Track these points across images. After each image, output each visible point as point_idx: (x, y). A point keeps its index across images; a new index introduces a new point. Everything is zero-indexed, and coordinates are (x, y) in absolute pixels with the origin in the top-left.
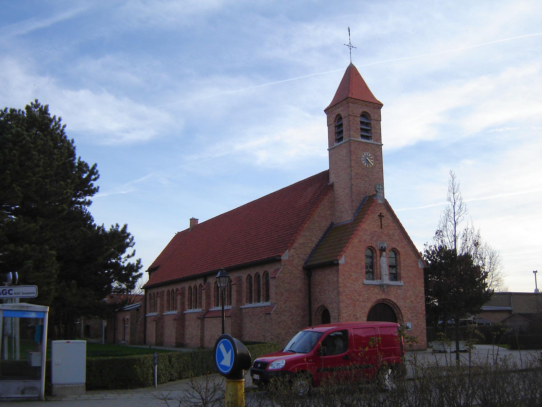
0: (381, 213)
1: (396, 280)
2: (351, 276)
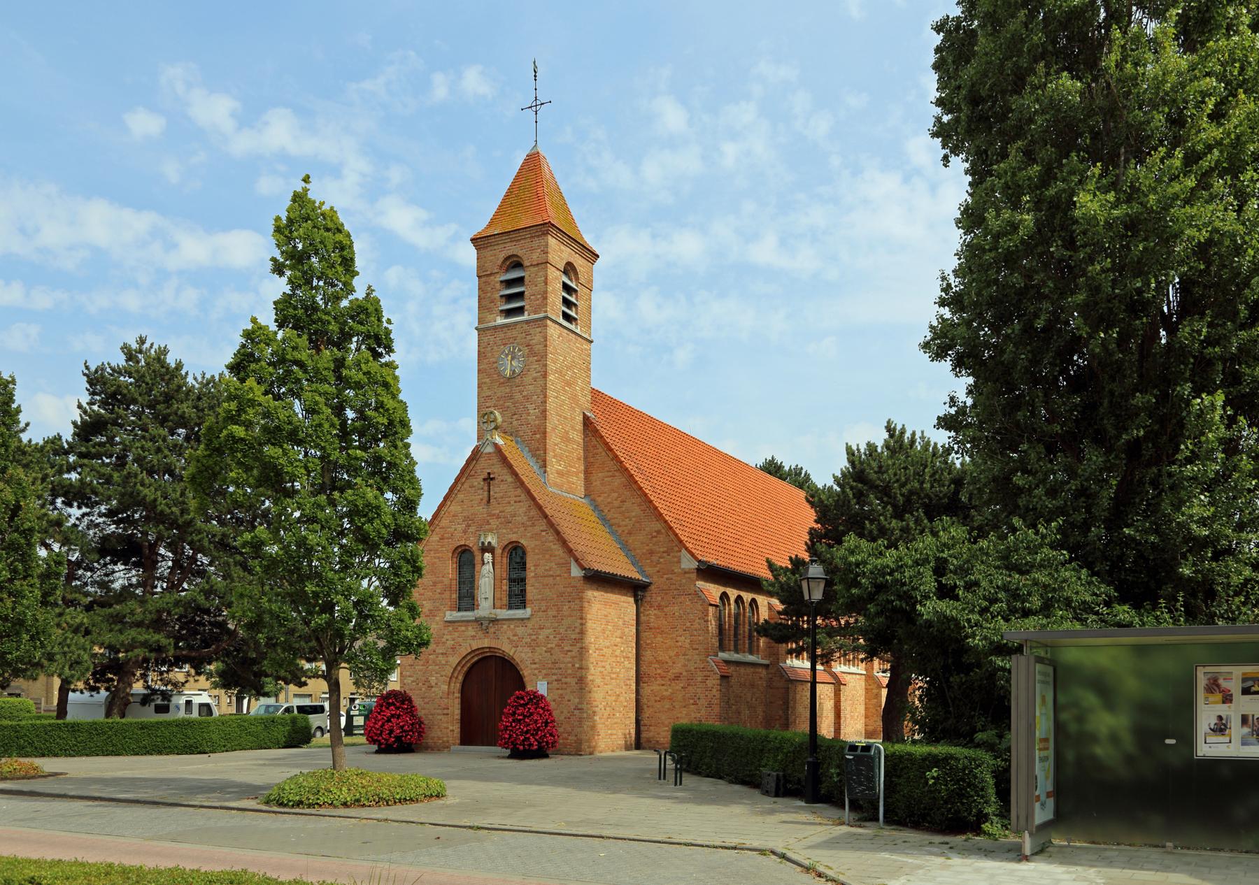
1: (518, 608)
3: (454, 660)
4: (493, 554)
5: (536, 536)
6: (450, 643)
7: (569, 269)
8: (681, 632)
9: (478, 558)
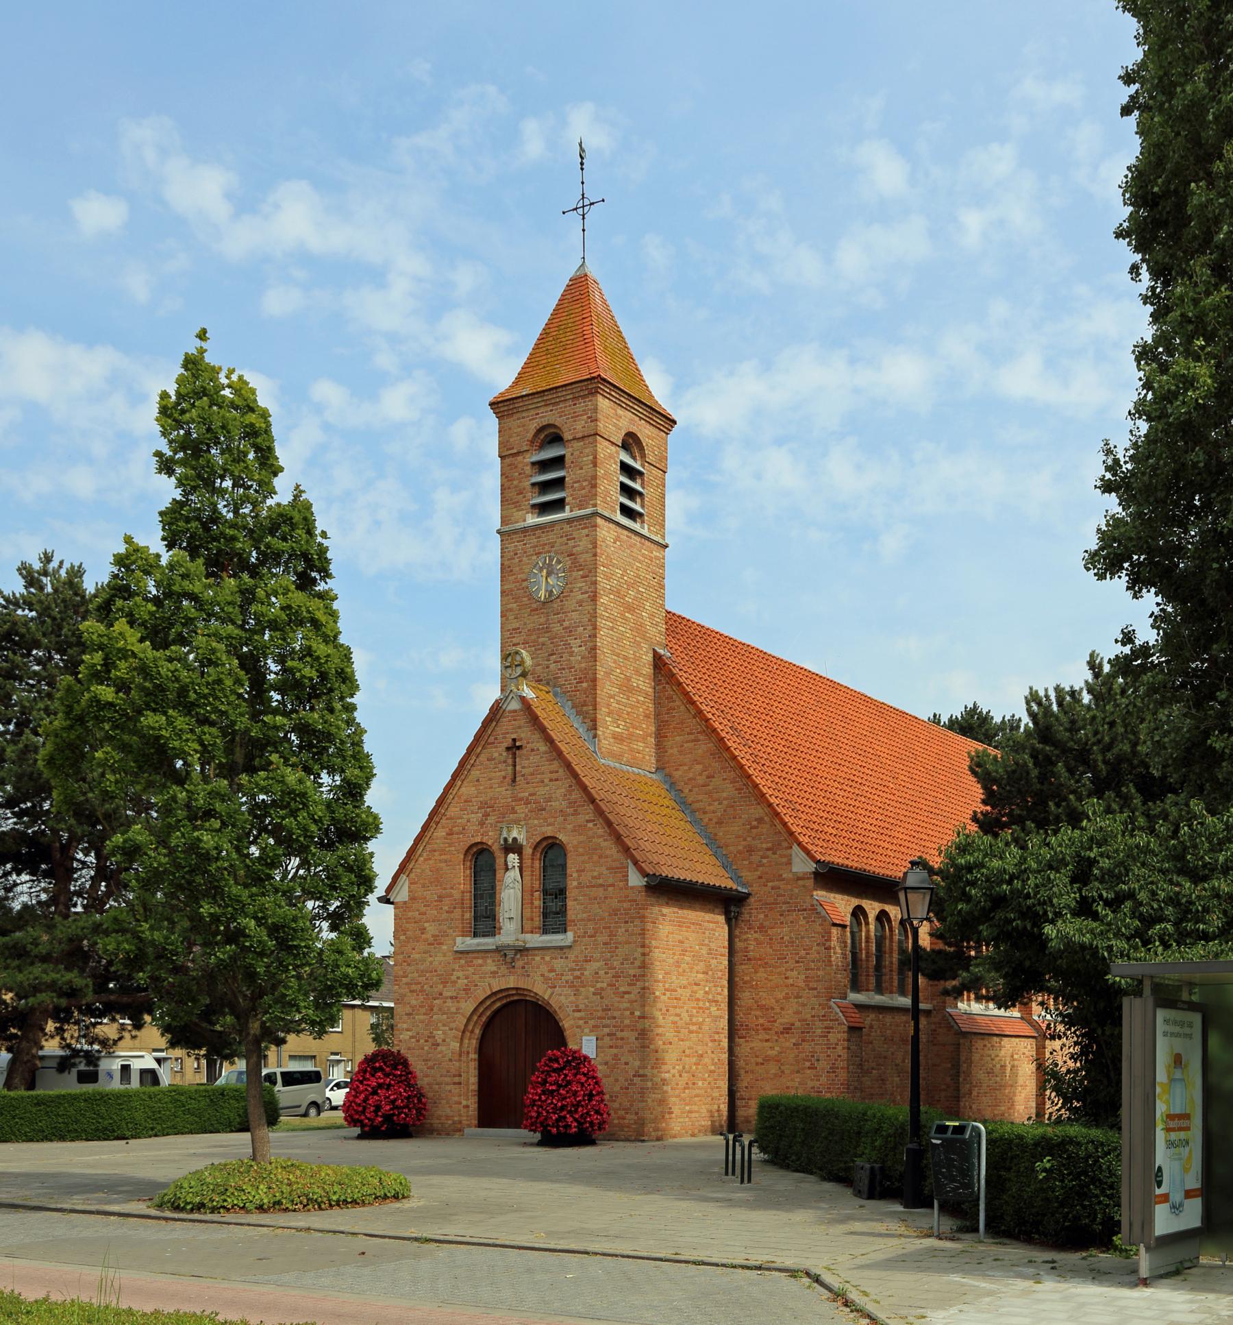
0: (514, 740)
1: (556, 932)
2: (423, 930)
3: (468, 1007)
4: (520, 854)
5: (579, 829)
7: (631, 442)
8: (792, 964)
9: (500, 861)
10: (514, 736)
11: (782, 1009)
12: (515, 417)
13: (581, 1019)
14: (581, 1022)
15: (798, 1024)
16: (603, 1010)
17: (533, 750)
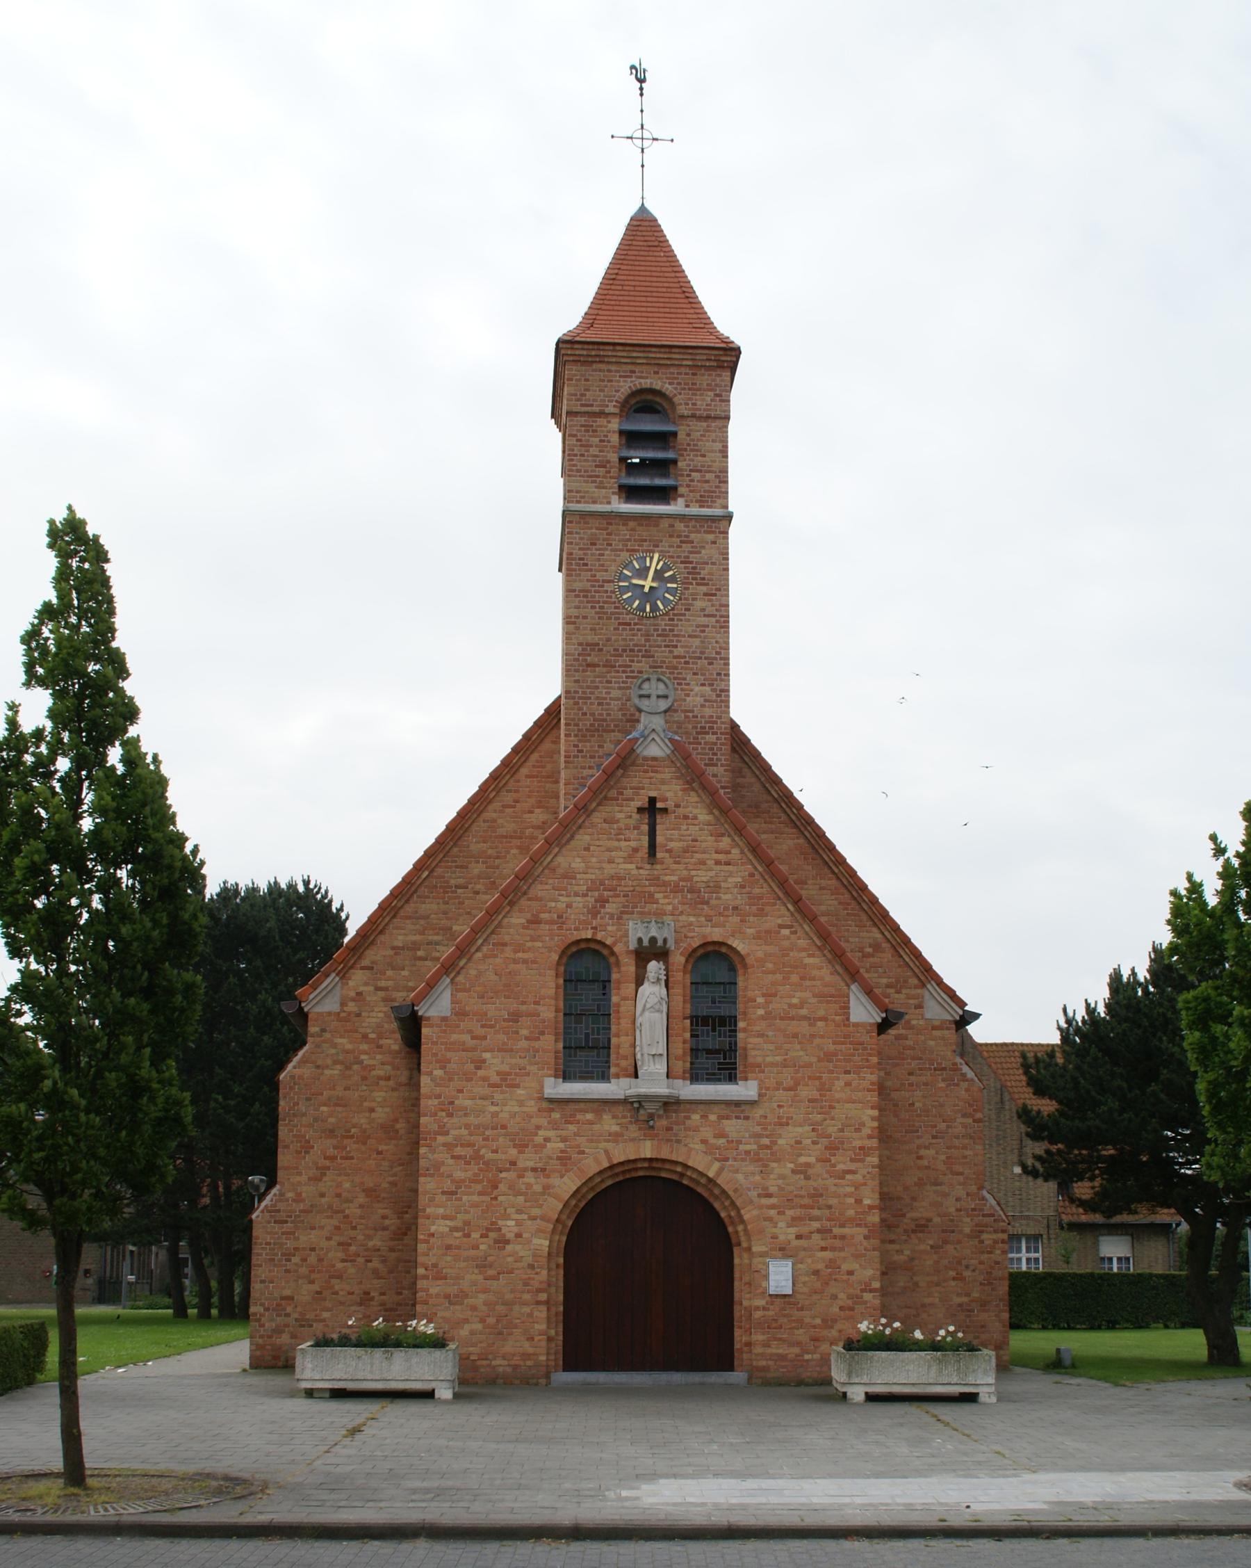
0: (652, 801)
2: (480, 1063)
3: (567, 1185)
5: (765, 936)
6: (555, 1146)
10: (653, 794)
11: (914, 1199)
12: (595, 366)
13: (772, 1207)
14: (773, 1212)
15: (937, 1220)
16: (811, 1196)
17: (686, 817)
